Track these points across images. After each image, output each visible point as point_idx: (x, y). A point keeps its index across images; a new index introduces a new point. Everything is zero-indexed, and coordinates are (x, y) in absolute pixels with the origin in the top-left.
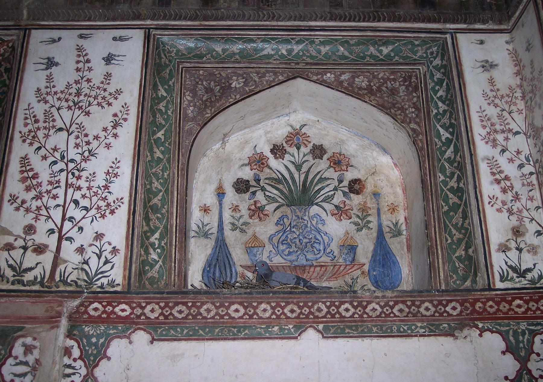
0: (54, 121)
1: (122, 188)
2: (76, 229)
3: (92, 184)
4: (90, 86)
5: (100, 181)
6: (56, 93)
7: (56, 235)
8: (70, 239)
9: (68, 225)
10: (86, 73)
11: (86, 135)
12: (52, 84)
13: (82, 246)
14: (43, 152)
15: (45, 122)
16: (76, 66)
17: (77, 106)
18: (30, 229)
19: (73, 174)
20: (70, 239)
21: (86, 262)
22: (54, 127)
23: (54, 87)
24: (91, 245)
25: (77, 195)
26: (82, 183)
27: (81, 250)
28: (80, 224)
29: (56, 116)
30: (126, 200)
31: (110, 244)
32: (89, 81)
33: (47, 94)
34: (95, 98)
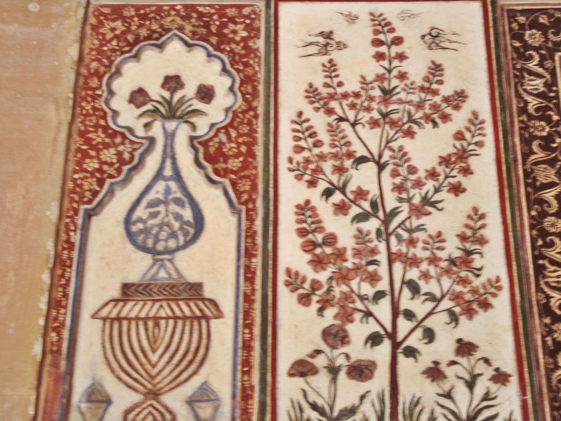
0: (348, 144)
1: (493, 262)
2: (419, 333)
3: (439, 254)
4: (406, 85)
5: (452, 248)
6: (345, 96)
7: (386, 345)
8: (411, 352)
9: (404, 325)
10: (396, 63)
11: (412, 170)
12: (336, 80)
13: (436, 363)
14: (337, 197)
15: (333, 146)
16: (374, 50)
17: (387, 120)
18: (335, 336)
19: (399, 237)
20: (411, 352)
21: (448, 395)
22: (350, 155)
23: (340, 84)
24: (453, 363)
25: (413, 274)
26: (419, 252)
27: (434, 373)
28: (428, 323)
29: (352, 137)
30: (505, 282)
31: (487, 361)
32: (402, 76)
33: (332, 97)
34: (420, 106)
